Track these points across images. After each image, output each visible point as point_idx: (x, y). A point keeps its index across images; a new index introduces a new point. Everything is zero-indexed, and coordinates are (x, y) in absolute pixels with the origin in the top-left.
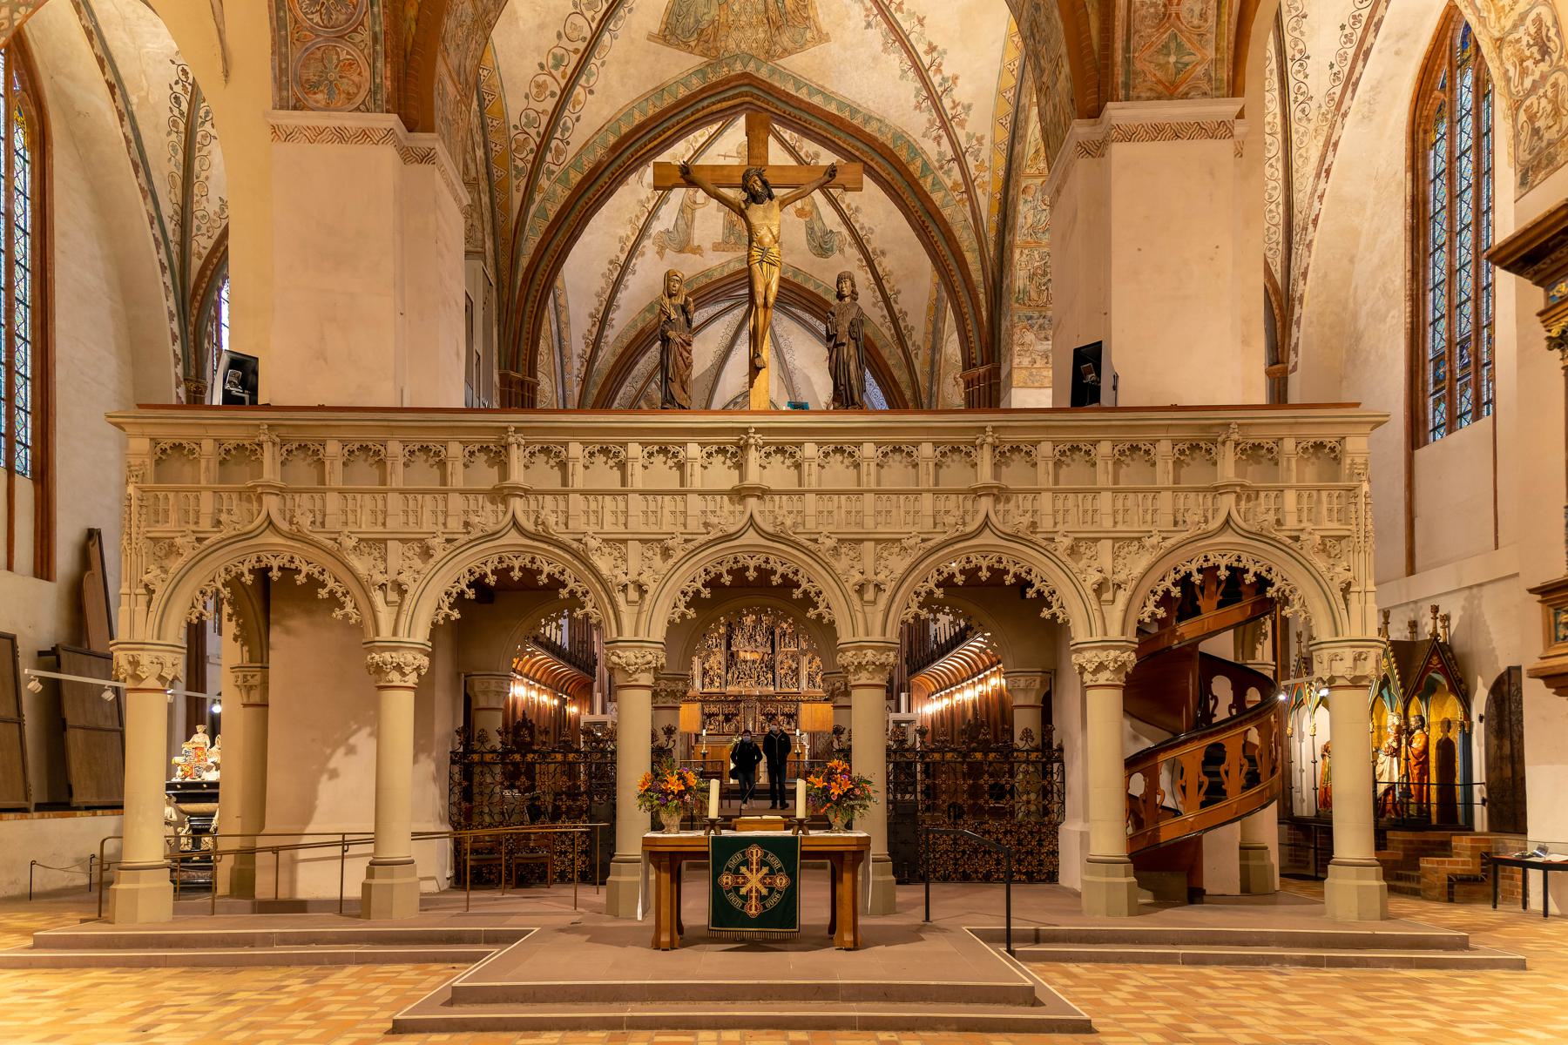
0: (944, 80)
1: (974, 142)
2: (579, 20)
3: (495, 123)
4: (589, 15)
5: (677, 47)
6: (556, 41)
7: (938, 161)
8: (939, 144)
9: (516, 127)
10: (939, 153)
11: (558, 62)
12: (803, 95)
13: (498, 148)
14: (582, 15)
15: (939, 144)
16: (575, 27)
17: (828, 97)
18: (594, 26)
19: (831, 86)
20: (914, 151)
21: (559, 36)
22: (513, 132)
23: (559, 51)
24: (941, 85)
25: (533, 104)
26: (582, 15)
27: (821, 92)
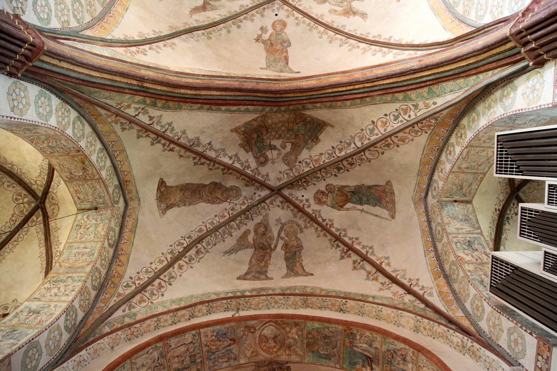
0: (159, 142)
1: (127, 127)
2: (370, 157)
3: (438, 138)
4: (364, 157)
5: (318, 119)
6: (385, 152)
7: (147, 110)
8: (150, 117)
9: (426, 133)
10: (148, 113)
11: (388, 145)
12: (243, 108)
13: (443, 130)
14: (367, 158)
15: (150, 117)
17: (226, 111)
18: (363, 153)
19: (228, 115)
20: (164, 108)
21: (383, 153)
22: (429, 132)
24: (160, 140)
25: (411, 137)
27: (234, 111)
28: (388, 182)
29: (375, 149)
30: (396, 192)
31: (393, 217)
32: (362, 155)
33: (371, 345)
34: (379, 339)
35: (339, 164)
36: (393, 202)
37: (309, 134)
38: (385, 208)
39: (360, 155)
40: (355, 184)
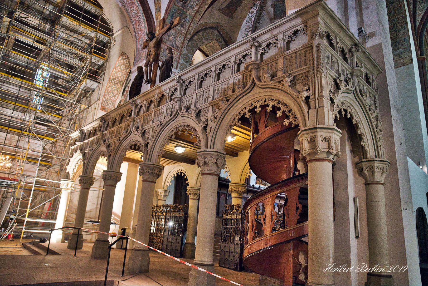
2: (249, 24)
4: (250, 22)
14: (249, 22)
16: (248, 26)
18: (252, 24)
21: (245, 29)
23: (246, 33)
26: (249, 22)
28: (232, 17)
29: (249, 30)
30: (227, 17)
31: (219, 10)
32: (252, 22)
33: (191, 7)
34: (192, 13)
35: (257, 8)
36: (224, 13)
37: (278, 6)
38: (223, 9)
39: (253, 21)
40: (243, 3)
